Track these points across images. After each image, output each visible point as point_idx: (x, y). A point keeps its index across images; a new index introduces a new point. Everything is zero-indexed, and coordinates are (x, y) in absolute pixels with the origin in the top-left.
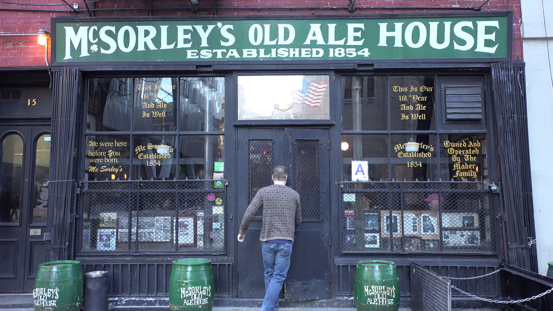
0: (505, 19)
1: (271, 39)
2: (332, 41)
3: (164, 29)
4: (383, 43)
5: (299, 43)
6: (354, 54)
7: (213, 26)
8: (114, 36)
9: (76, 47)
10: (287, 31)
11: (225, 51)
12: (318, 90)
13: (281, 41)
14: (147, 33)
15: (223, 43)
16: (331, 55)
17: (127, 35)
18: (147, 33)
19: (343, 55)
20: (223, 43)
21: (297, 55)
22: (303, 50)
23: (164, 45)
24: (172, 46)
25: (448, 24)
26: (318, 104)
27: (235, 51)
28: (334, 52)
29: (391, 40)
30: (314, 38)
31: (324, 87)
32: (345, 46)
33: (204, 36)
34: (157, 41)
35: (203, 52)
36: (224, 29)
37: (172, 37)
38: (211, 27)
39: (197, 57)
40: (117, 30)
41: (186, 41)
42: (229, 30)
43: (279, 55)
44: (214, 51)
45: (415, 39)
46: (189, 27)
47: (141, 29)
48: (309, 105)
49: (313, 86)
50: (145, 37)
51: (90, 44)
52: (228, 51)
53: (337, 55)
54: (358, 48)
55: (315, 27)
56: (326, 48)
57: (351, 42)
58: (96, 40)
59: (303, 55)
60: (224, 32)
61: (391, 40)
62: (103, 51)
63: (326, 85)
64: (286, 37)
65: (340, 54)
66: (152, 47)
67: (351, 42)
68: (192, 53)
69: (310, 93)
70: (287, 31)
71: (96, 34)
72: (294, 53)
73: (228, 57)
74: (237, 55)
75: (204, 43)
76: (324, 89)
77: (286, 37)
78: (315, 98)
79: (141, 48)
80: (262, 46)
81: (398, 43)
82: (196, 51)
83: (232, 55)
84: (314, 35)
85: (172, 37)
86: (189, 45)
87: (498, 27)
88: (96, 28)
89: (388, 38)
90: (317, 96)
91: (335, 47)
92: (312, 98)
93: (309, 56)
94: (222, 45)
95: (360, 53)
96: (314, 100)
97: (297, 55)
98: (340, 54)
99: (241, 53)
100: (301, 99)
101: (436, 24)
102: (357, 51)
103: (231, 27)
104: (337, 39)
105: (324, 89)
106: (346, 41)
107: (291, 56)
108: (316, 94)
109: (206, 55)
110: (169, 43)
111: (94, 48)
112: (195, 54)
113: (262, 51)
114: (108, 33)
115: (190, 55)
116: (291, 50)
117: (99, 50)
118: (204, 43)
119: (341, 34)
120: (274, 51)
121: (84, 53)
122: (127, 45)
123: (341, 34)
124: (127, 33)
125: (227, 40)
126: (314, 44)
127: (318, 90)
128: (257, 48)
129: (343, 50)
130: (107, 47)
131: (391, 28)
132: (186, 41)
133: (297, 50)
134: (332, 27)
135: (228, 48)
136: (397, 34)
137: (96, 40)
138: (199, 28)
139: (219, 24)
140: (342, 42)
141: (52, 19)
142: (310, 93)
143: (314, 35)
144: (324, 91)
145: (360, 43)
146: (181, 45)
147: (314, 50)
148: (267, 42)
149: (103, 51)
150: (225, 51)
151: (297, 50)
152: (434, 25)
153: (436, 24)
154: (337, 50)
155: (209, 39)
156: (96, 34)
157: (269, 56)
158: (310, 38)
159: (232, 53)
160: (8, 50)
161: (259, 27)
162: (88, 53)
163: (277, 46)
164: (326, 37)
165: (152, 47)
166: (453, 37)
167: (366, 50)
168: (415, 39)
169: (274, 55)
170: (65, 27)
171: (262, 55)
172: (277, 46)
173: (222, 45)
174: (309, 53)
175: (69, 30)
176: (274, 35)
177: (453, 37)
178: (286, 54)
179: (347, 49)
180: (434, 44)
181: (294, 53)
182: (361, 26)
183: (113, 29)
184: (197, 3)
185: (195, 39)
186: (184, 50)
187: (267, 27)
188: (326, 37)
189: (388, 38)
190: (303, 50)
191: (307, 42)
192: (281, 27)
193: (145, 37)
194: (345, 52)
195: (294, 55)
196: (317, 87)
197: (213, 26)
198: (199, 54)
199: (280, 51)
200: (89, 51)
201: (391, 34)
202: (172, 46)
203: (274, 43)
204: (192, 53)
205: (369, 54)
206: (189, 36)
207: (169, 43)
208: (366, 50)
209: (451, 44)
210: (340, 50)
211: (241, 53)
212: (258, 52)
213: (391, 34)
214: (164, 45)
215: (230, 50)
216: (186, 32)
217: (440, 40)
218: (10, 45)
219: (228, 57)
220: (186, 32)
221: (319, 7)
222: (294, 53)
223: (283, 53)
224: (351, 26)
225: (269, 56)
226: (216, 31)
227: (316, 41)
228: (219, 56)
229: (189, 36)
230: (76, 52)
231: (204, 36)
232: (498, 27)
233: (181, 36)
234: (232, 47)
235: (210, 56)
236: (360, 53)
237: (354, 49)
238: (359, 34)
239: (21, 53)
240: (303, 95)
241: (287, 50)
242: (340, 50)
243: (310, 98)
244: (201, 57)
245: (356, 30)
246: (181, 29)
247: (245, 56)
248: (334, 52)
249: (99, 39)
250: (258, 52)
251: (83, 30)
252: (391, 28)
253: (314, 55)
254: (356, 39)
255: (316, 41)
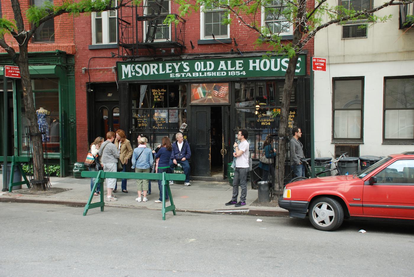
0: (304, 57)
1: (204, 68)
2: (229, 68)
3: (161, 65)
4: (251, 69)
5: (215, 70)
6: (239, 74)
7: (180, 63)
8: (141, 69)
9: (126, 74)
10: (210, 65)
11: (185, 74)
12: (224, 90)
13: (208, 69)
14: (154, 67)
15: (184, 71)
16: (229, 75)
17: (146, 67)
18: (154, 67)
19: (234, 74)
20: (184, 71)
21: (215, 75)
22: (218, 73)
23: (161, 72)
24: (164, 72)
25: (279, 60)
26: (224, 96)
27: (189, 74)
28: (231, 73)
29: (254, 67)
30: (222, 67)
31: (227, 89)
32: (235, 71)
33: (177, 68)
34: (158, 70)
35: (177, 75)
36: (185, 65)
37: (164, 69)
38: (179, 64)
39: (174, 77)
40: (142, 66)
41: (170, 70)
42: (187, 65)
43: (207, 75)
44: (181, 74)
45: (265, 66)
46: (171, 64)
47: (152, 65)
48: (220, 96)
49: (222, 88)
50: (153, 68)
51: (132, 72)
52: (187, 74)
53: (232, 74)
54: (241, 71)
55: (222, 63)
56: (227, 71)
57: (238, 69)
58: (134, 70)
59: (218, 75)
60: (185, 66)
61: (254, 67)
62: (137, 75)
63: (227, 88)
64: (210, 67)
65: (233, 74)
66: (156, 73)
67: (238, 69)
68: (172, 75)
69: (221, 91)
70: (210, 64)
71: (134, 68)
72: (214, 74)
73: (186, 76)
74: (190, 76)
75: (177, 71)
76: (227, 89)
77: (210, 67)
78: (222, 93)
79: (152, 73)
80: (200, 71)
81: (258, 69)
82: (174, 74)
83: (188, 75)
84: (222, 66)
85: (164, 69)
86: (171, 72)
87: (301, 61)
88: (134, 65)
89: (253, 66)
90: (224, 92)
91: (231, 71)
92: (221, 93)
93: (220, 75)
94: (184, 71)
95: (241, 73)
96: (222, 94)
97: (215, 75)
98: (233, 74)
99: (192, 75)
100: (217, 94)
101: (274, 60)
102: (240, 73)
103: (188, 63)
104: (231, 67)
105: (227, 89)
106: (236, 68)
107: (213, 75)
108: (223, 92)
109: (178, 75)
110: (163, 71)
111: (134, 74)
112: (174, 75)
113: (201, 73)
114: (139, 67)
115: (171, 76)
116: (213, 73)
117: (135, 75)
118: (177, 71)
119: (233, 65)
120: (205, 73)
121: (130, 76)
122: (146, 72)
123: (233, 65)
124: (146, 67)
125: (186, 69)
126: (222, 70)
127: (224, 90)
128: (199, 72)
129: (234, 72)
130: (138, 73)
131: (254, 62)
132: (170, 70)
133: (215, 73)
134: (229, 62)
135: (186, 73)
136: (257, 65)
137: (134, 70)
138: (175, 64)
139: (183, 62)
140: (234, 69)
141: (117, 63)
142: (221, 91)
143: (222, 66)
144: (226, 90)
145: (241, 69)
146: (168, 72)
147: (222, 73)
148: (203, 70)
149: (137, 75)
150: (185, 74)
151: (215, 73)
152: (273, 61)
153: (274, 60)
154: (232, 72)
155: (179, 69)
156: (134, 68)
157: (203, 76)
158: (220, 67)
159: (188, 74)
160: (101, 74)
161: (199, 63)
162: (131, 76)
163: (207, 71)
164: (227, 67)
165: (156, 73)
166: (281, 65)
167: (244, 72)
168: (265, 66)
169: (205, 75)
170: (122, 65)
171: (201, 75)
172: (207, 71)
173: (184, 71)
174: (220, 74)
175: (123, 66)
176: (205, 67)
177: (281, 65)
178: (210, 75)
179: (236, 72)
180: (273, 69)
181: (214, 74)
182: (242, 61)
183: (140, 65)
184: (174, 52)
185: (173, 69)
186: (169, 74)
187: (202, 63)
188: (227, 67)
189: (253, 66)
190: (218, 73)
191: (219, 69)
192: (208, 63)
193: (153, 68)
194: (235, 73)
195: (214, 75)
196: (223, 88)
197: (180, 63)
198: (175, 75)
199: (208, 73)
200: (132, 75)
201: (254, 65)
202: (164, 72)
203: (205, 70)
204: (172, 75)
205: (245, 73)
206: (171, 68)
207: (163, 71)
208: (244, 72)
209: (280, 69)
210: (233, 72)
211: (192, 75)
212: (199, 74)
213: (254, 65)
214: (161, 72)
215: (188, 73)
216: (169, 66)
217: (276, 67)
218: (101, 72)
219: (186, 76)
220: (169, 66)
221: (225, 52)
222: (214, 74)
223: (209, 74)
224: (237, 62)
225: (203, 76)
226: (182, 65)
227: (223, 69)
228: (183, 76)
229: (171, 68)
230: (127, 75)
231: (177, 68)
232: (301, 61)
233: (168, 68)
234: (188, 72)
235: (179, 76)
236: (241, 73)
237: (239, 72)
238: (241, 65)
239: (106, 76)
240: (218, 92)
241: (211, 73)
242: (233, 72)
243: (221, 93)
244: (176, 77)
245: (240, 63)
246: (167, 65)
247: (194, 76)
248: (231, 73)
249: (135, 70)
250: (199, 74)
251: (129, 66)
252: (254, 62)
253: (222, 75)
254: (240, 67)
255: (223, 69)
